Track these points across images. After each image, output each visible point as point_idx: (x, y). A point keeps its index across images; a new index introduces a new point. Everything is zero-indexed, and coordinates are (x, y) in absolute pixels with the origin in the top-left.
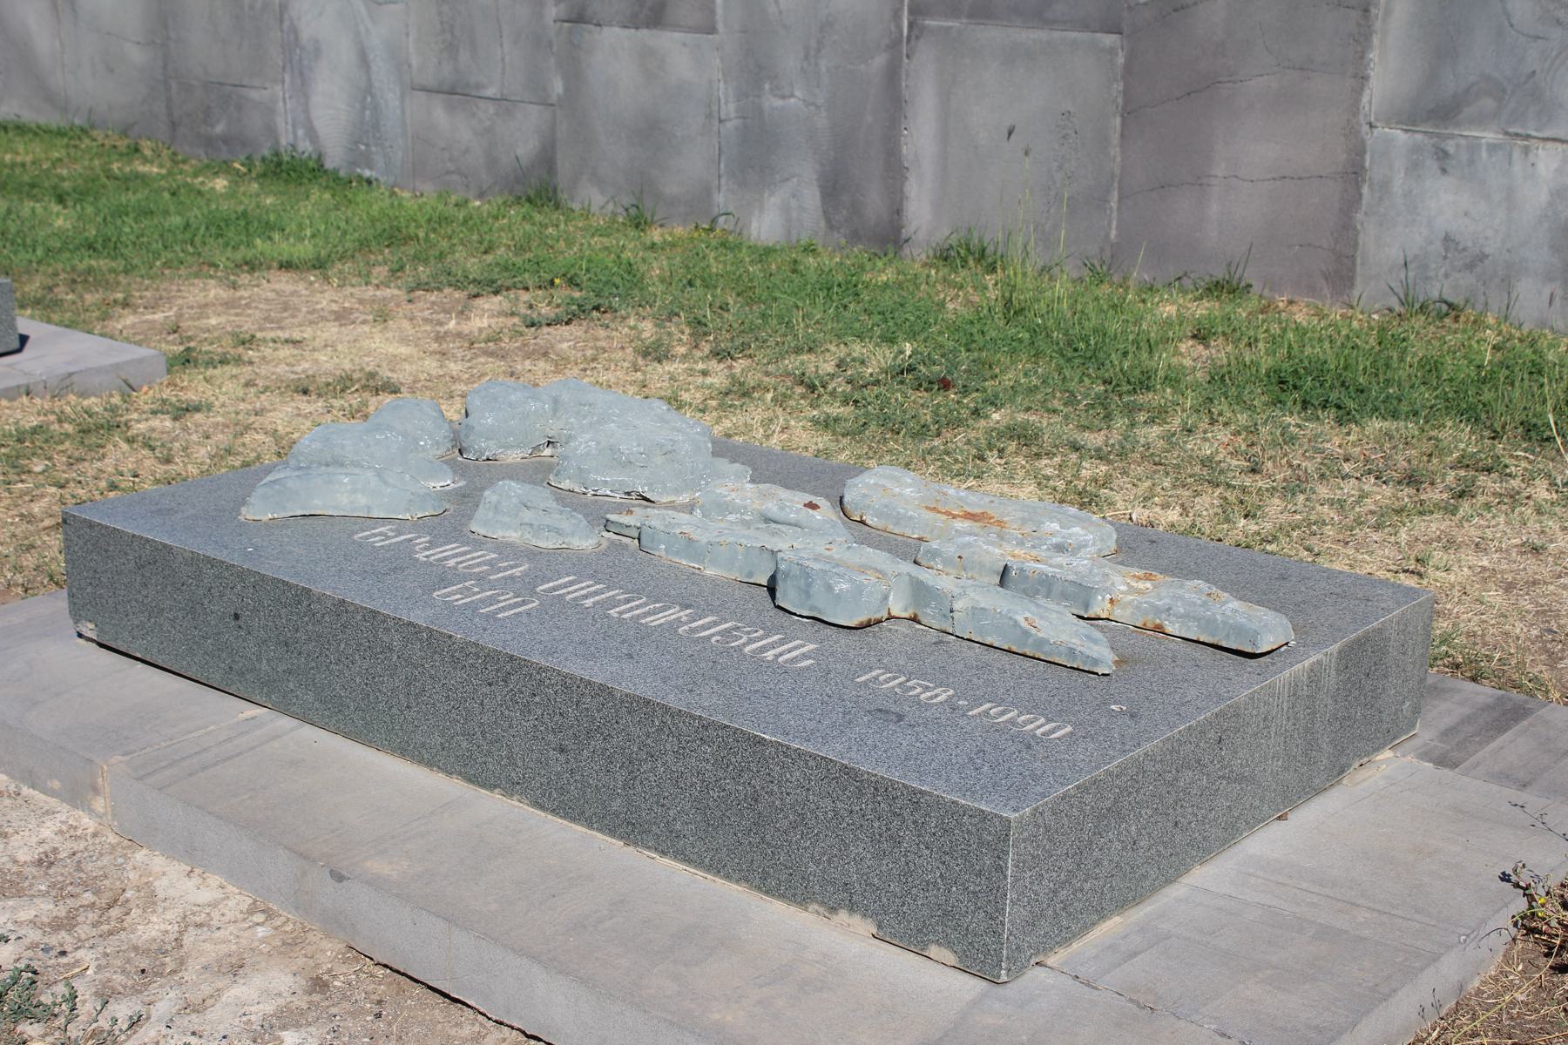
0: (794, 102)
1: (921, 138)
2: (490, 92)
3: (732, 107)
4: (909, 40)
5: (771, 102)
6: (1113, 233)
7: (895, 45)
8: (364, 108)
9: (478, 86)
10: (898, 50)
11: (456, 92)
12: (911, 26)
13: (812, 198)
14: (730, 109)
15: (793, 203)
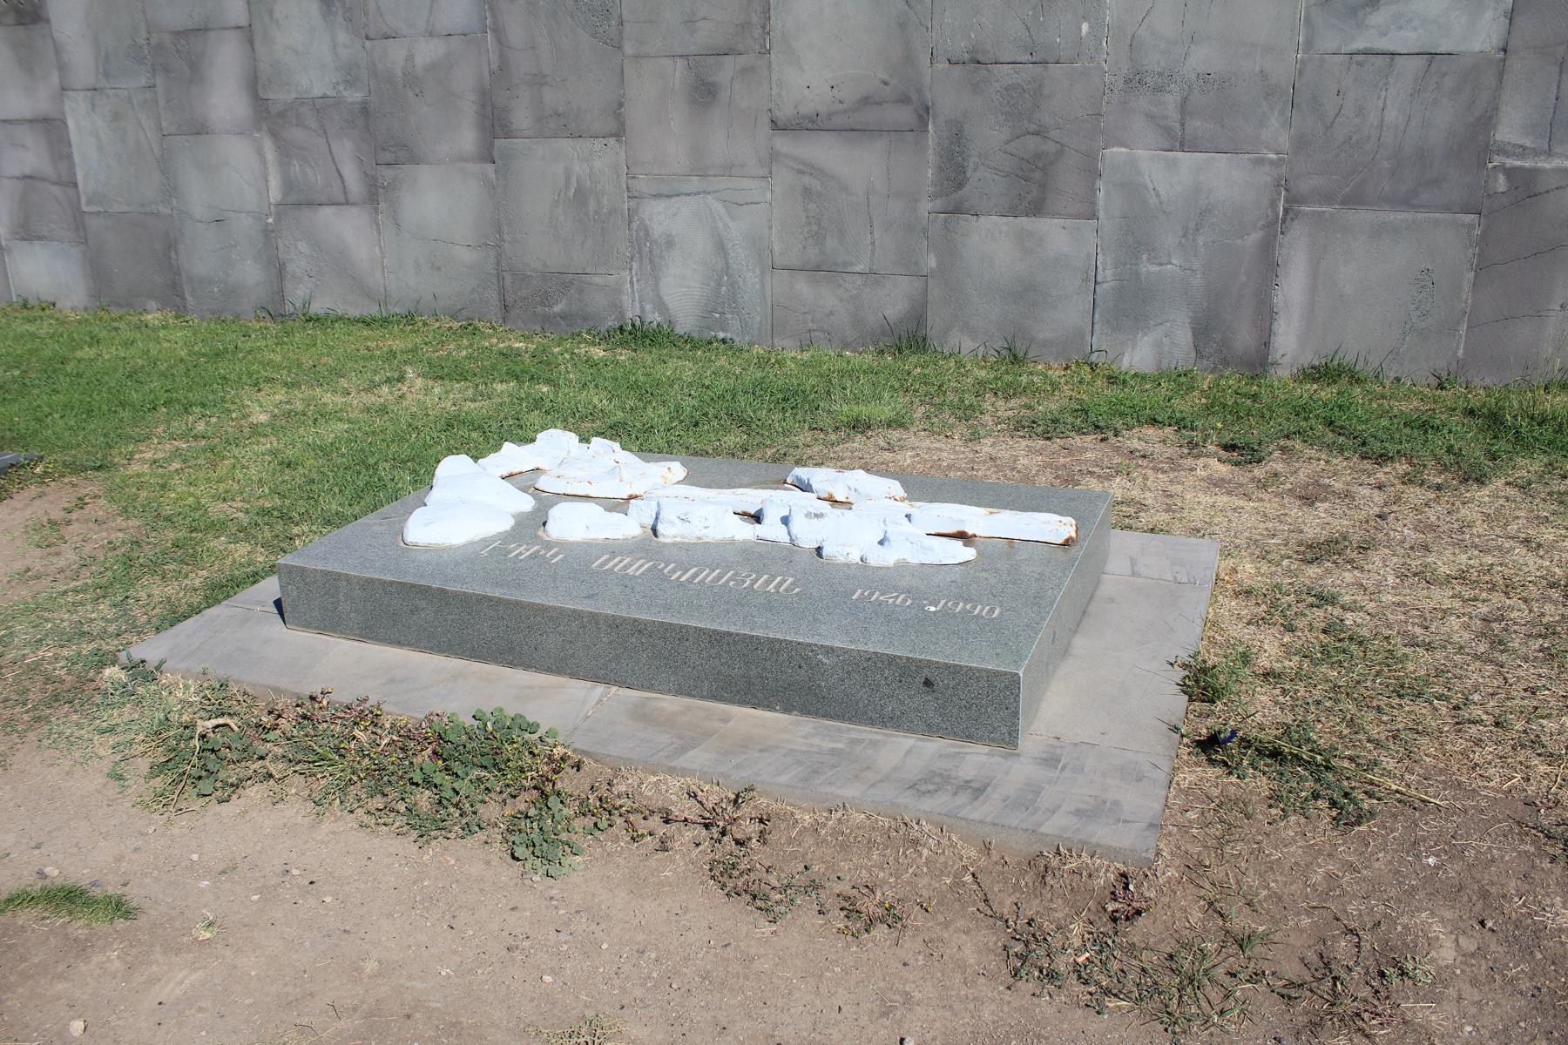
0: (1171, 265)
1: (1292, 289)
2: (857, 269)
3: (1109, 273)
4: (1284, 221)
5: (1148, 268)
6: (1460, 353)
7: (1270, 225)
8: (720, 285)
9: (845, 264)
10: (1275, 228)
11: (820, 270)
12: (1286, 211)
13: (1184, 337)
14: (1107, 274)
15: (1166, 341)
